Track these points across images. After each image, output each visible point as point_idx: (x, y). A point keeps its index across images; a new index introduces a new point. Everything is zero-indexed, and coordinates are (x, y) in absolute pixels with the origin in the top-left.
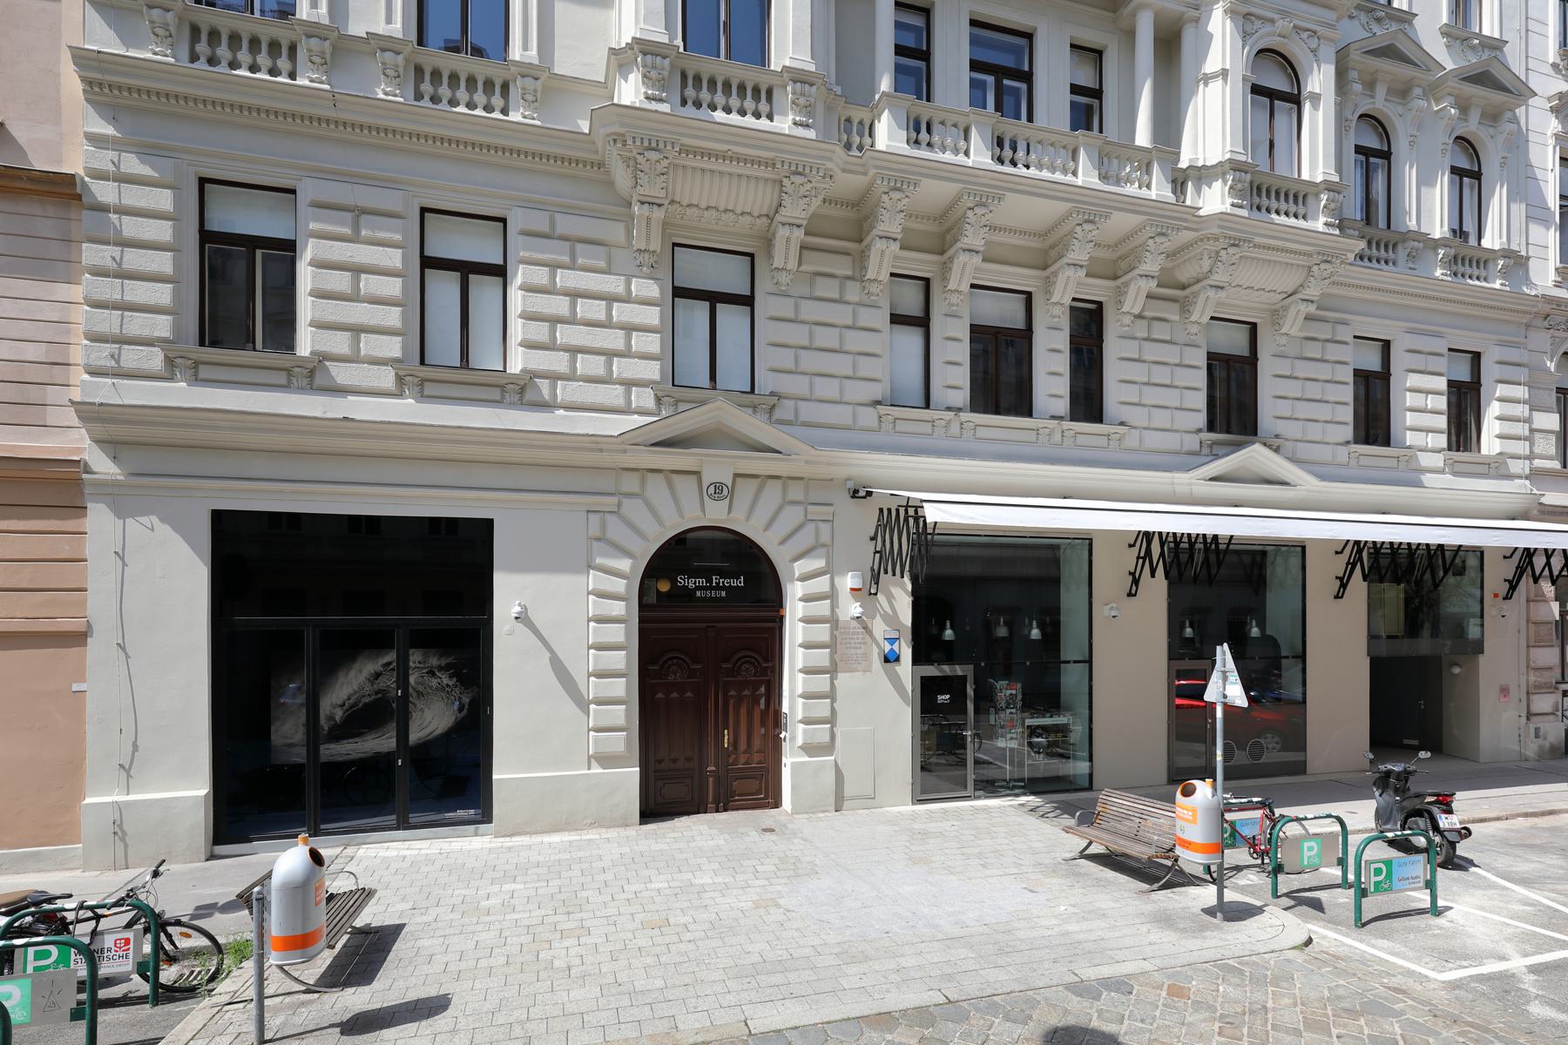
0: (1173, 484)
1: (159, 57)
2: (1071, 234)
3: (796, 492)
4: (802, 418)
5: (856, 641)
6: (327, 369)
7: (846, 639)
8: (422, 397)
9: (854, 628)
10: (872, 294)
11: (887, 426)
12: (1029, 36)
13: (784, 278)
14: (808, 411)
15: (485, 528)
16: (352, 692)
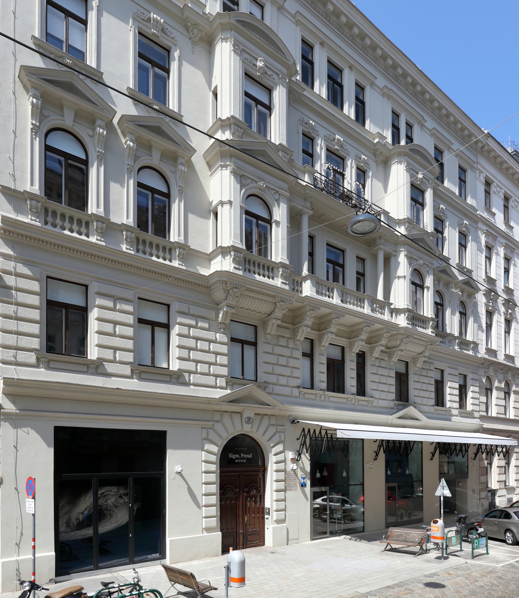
0: (387, 419)
1: (33, 222)
2: (362, 329)
3: (273, 421)
4: (275, 392)
6: (103, 365)
8: (140, 379)
10: (297, 345)
11: (302, 396)
12: (343, 251)
13: (269, 337)
14: (277, 389)
15: (162, 435)
16: (86, 506)
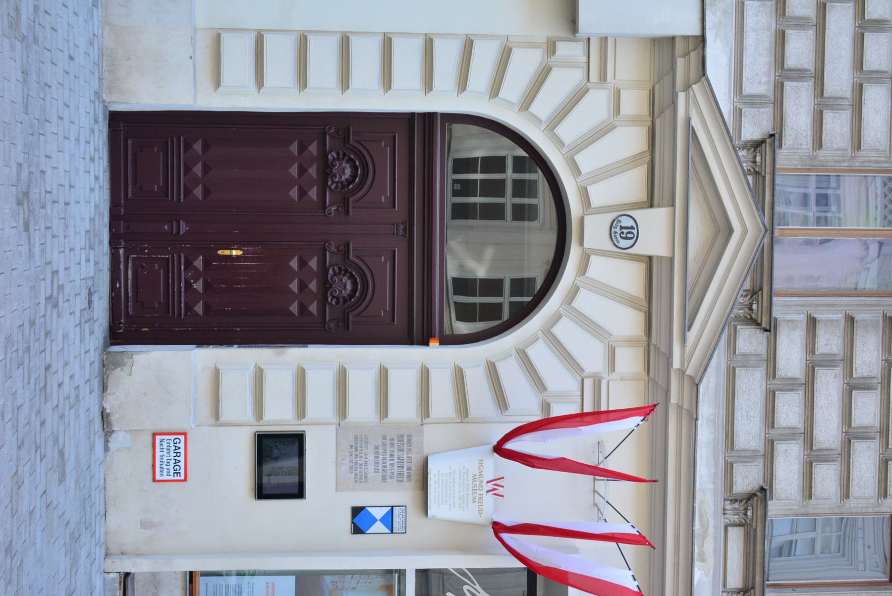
5: (388, 464)
7: (392, 445)
9: (409, 460)
